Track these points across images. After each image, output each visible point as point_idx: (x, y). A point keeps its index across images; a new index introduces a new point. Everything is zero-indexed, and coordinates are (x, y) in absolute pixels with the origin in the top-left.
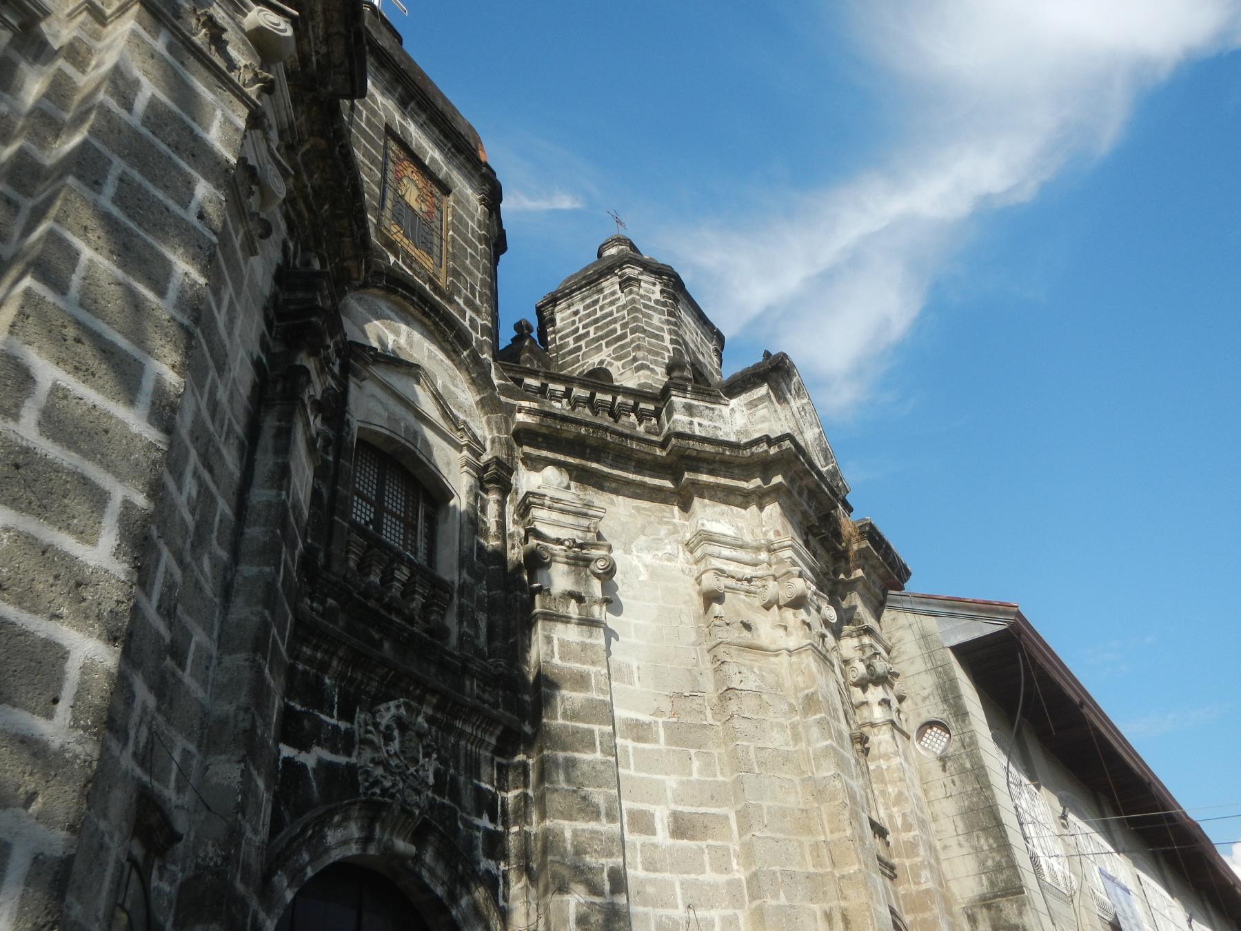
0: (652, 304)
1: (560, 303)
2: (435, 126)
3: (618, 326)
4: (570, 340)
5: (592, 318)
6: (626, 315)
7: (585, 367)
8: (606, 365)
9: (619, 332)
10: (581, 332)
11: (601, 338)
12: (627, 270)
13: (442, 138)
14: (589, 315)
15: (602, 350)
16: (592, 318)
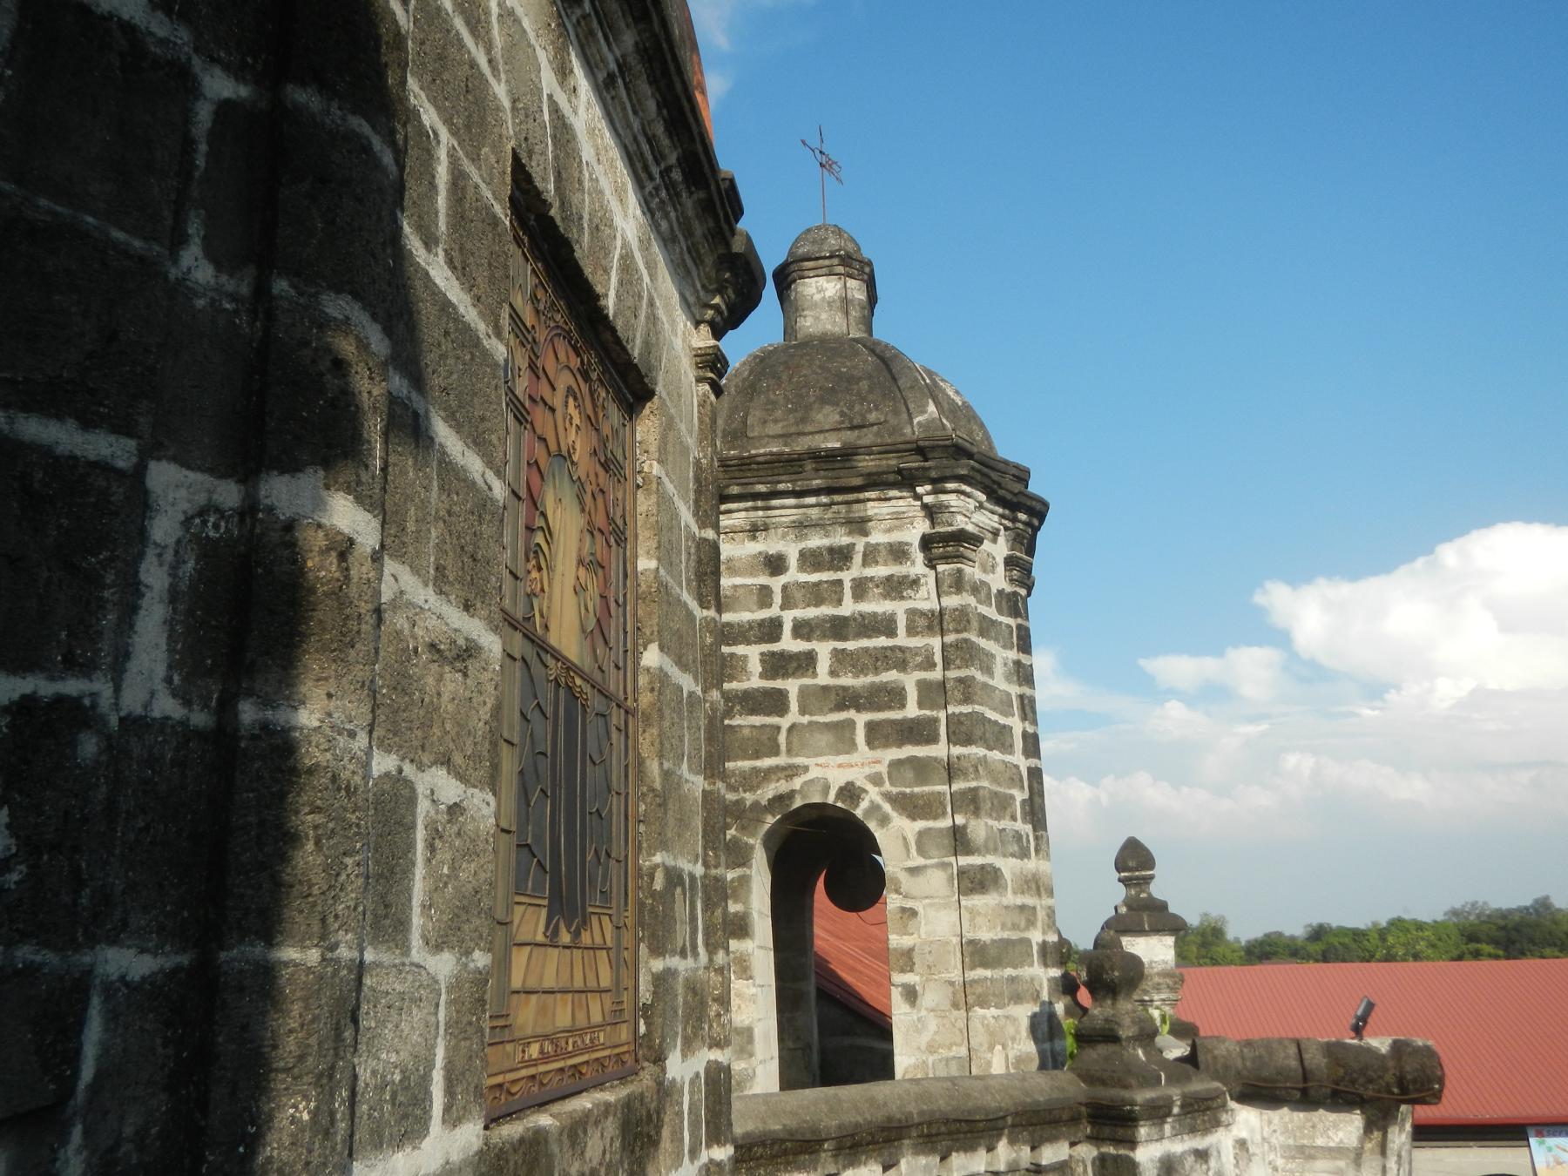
0: (991, 612)
1: (729, 512)
2: (653, 82)
3: (909, 681)
4: (752, 653)
5: (826, 610)
6: (938, 658)
7: (797, 783)
8: (868, 812)
9: (912, 710)
10: (789, 643)
11: (847, 699)
12: (951, 499)
13: (659, 129)
14: (816, 595)
15: (851, 746)
16: (826, 610)
